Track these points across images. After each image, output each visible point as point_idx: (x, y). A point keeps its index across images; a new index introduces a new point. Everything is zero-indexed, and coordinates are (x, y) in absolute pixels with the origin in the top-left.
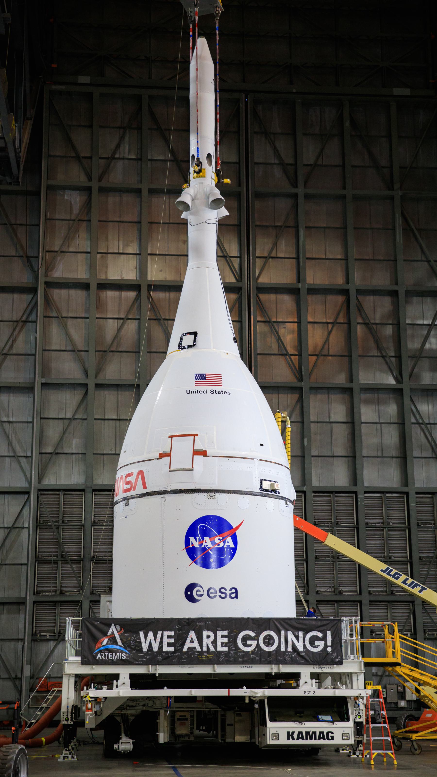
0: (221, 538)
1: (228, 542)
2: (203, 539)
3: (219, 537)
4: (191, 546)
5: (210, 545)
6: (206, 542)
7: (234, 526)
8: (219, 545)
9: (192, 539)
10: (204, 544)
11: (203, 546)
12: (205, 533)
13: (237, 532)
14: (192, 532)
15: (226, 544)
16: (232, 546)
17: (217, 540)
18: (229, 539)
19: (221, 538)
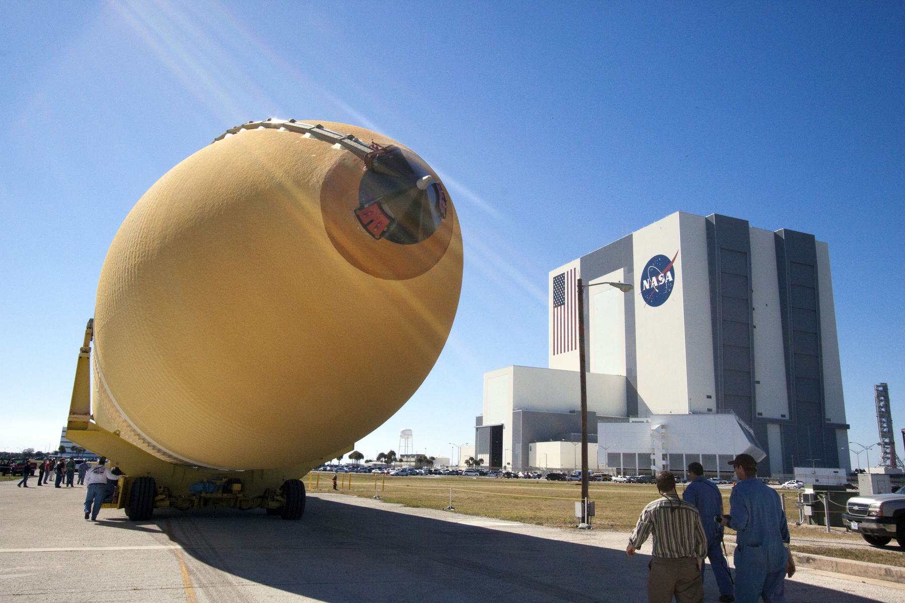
5: (656, 284)
9: (645, 282)
13: (674, 265)
16: (671, 279)
17: (660, 278)
18: (669, 274)
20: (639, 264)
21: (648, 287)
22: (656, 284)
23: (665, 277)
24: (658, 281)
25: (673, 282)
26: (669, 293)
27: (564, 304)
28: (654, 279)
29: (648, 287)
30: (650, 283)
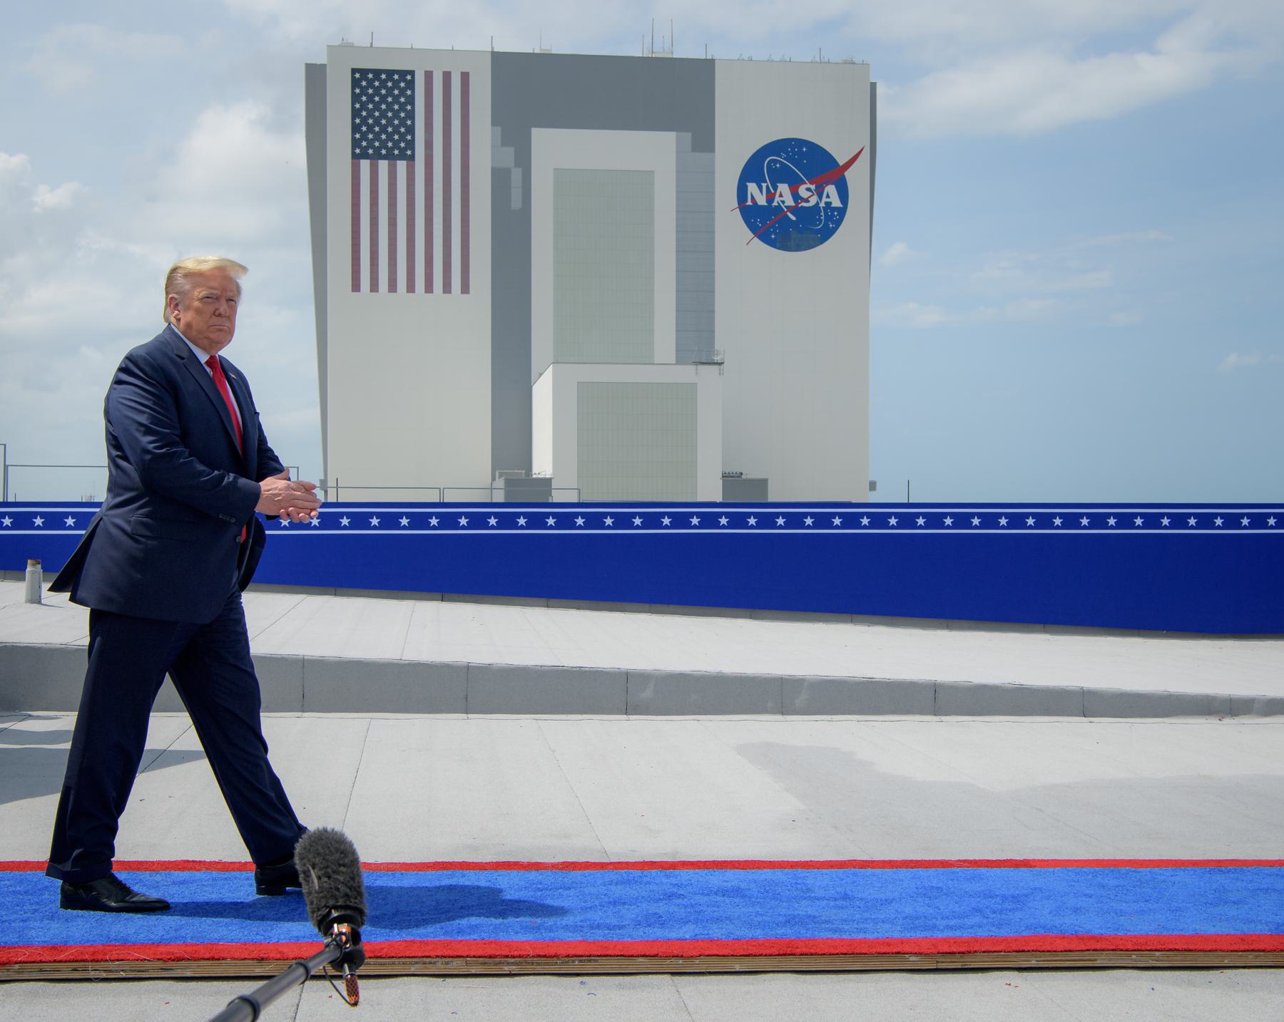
0: (813, 187)
1: (828, 196)
2: (775, 188)
3: (808, 185)
4: (749, 203)
5: (789, 201)
6: (781, 196)
7: (841, 162)
8: (807, 200)
9: (752, 188)
10: (777, 199)
11: (775, 204)
12: (780, 175)
14: (752, 171)
15: (824, 199)
16: (836, 203)
17: (802, 191)
18: (831, 190)
19: (813, 187)
20: (736, 143)
21: (762, 201)
22: (792, 203)
23: (820, 193)
24: (796, 196)
25: (842, 212)
26: (826, 234)
27: (412, 158)
28: (784, 188)
29: (762, 201)
30: (770, 198)
